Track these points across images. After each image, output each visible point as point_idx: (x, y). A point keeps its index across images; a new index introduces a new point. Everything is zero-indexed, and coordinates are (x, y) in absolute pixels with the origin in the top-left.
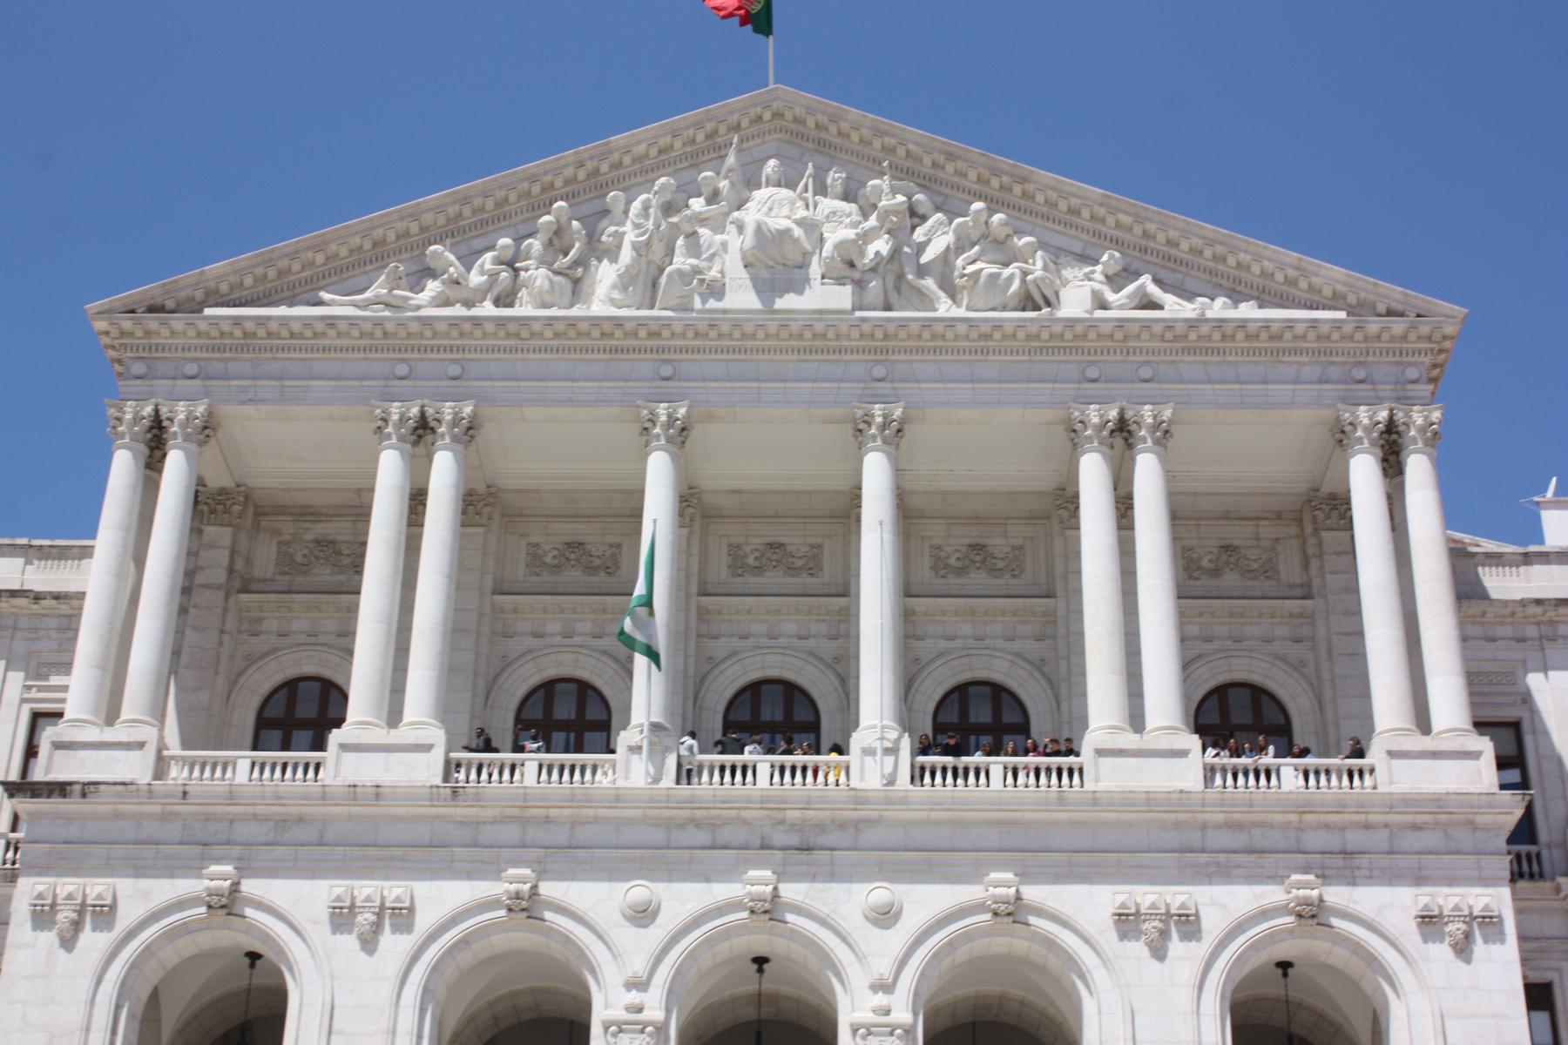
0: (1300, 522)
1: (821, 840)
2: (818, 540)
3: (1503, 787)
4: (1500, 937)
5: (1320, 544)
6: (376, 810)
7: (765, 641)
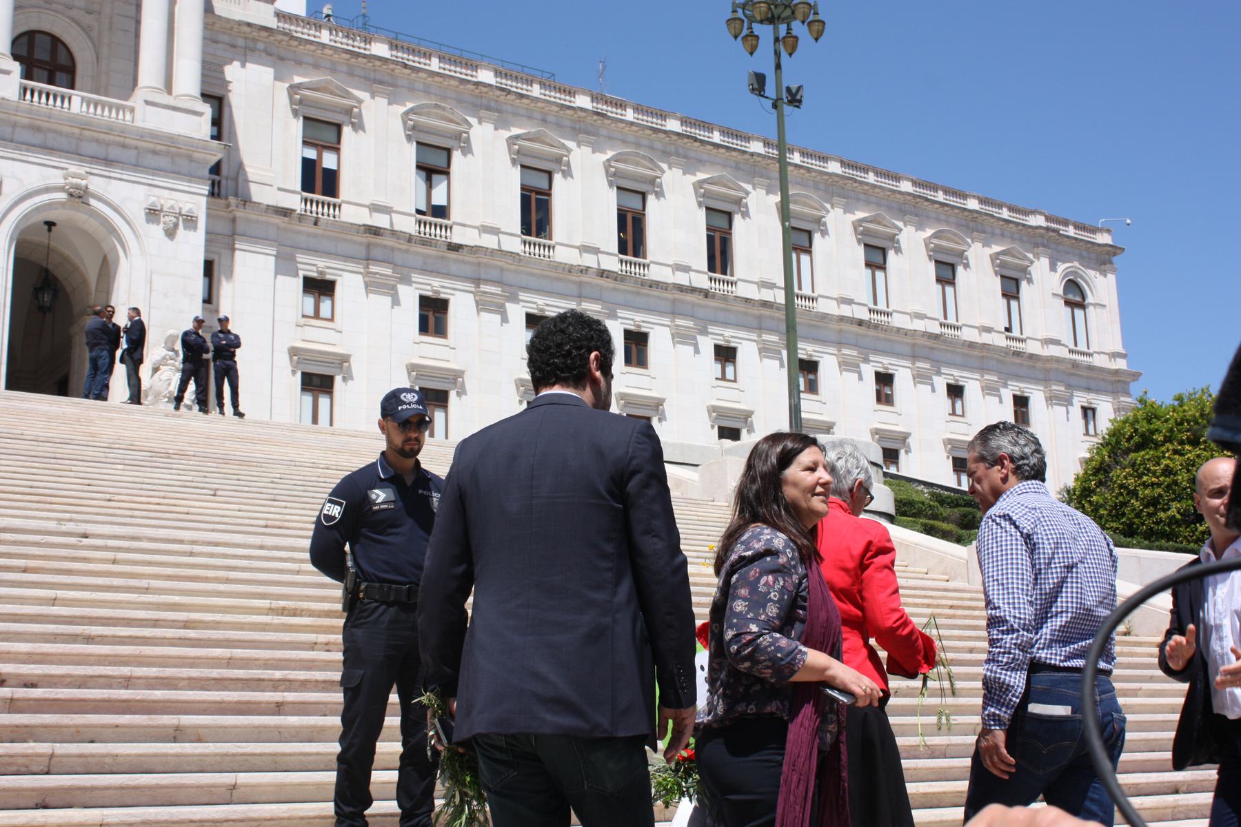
3: (213, 137)
4: (195, 228)
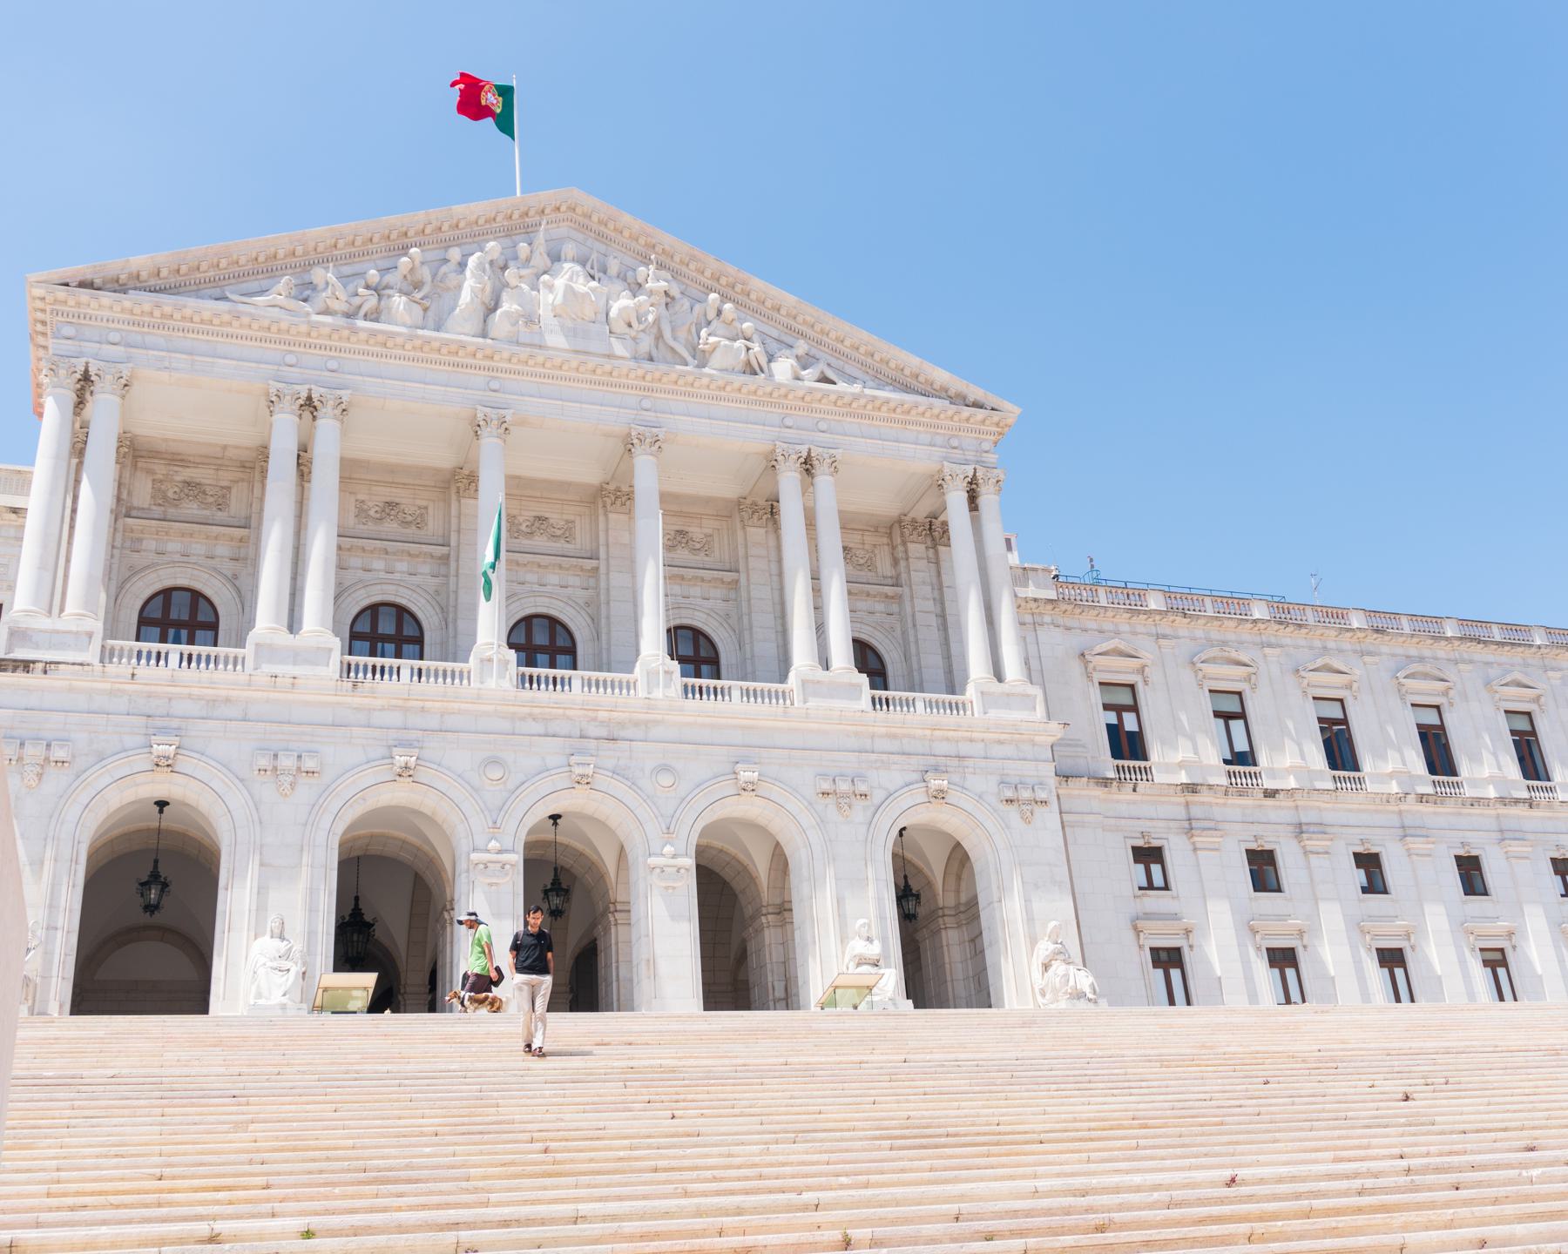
0: (890, 535)
1: (623, 734)
2: (571, 518)
5: (906, 551)
6: (290, 696)
7: (536, 588)
